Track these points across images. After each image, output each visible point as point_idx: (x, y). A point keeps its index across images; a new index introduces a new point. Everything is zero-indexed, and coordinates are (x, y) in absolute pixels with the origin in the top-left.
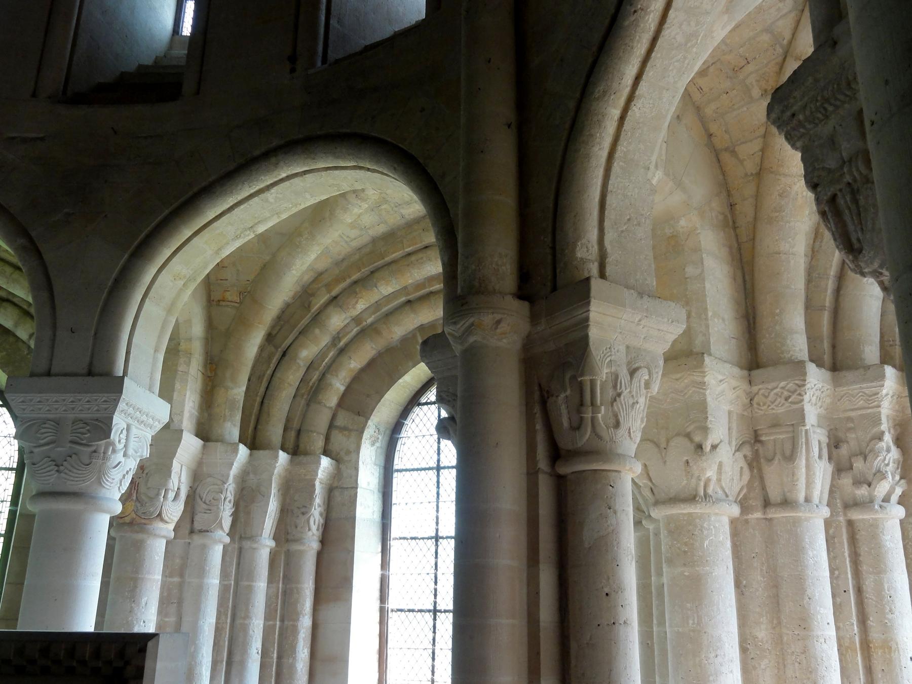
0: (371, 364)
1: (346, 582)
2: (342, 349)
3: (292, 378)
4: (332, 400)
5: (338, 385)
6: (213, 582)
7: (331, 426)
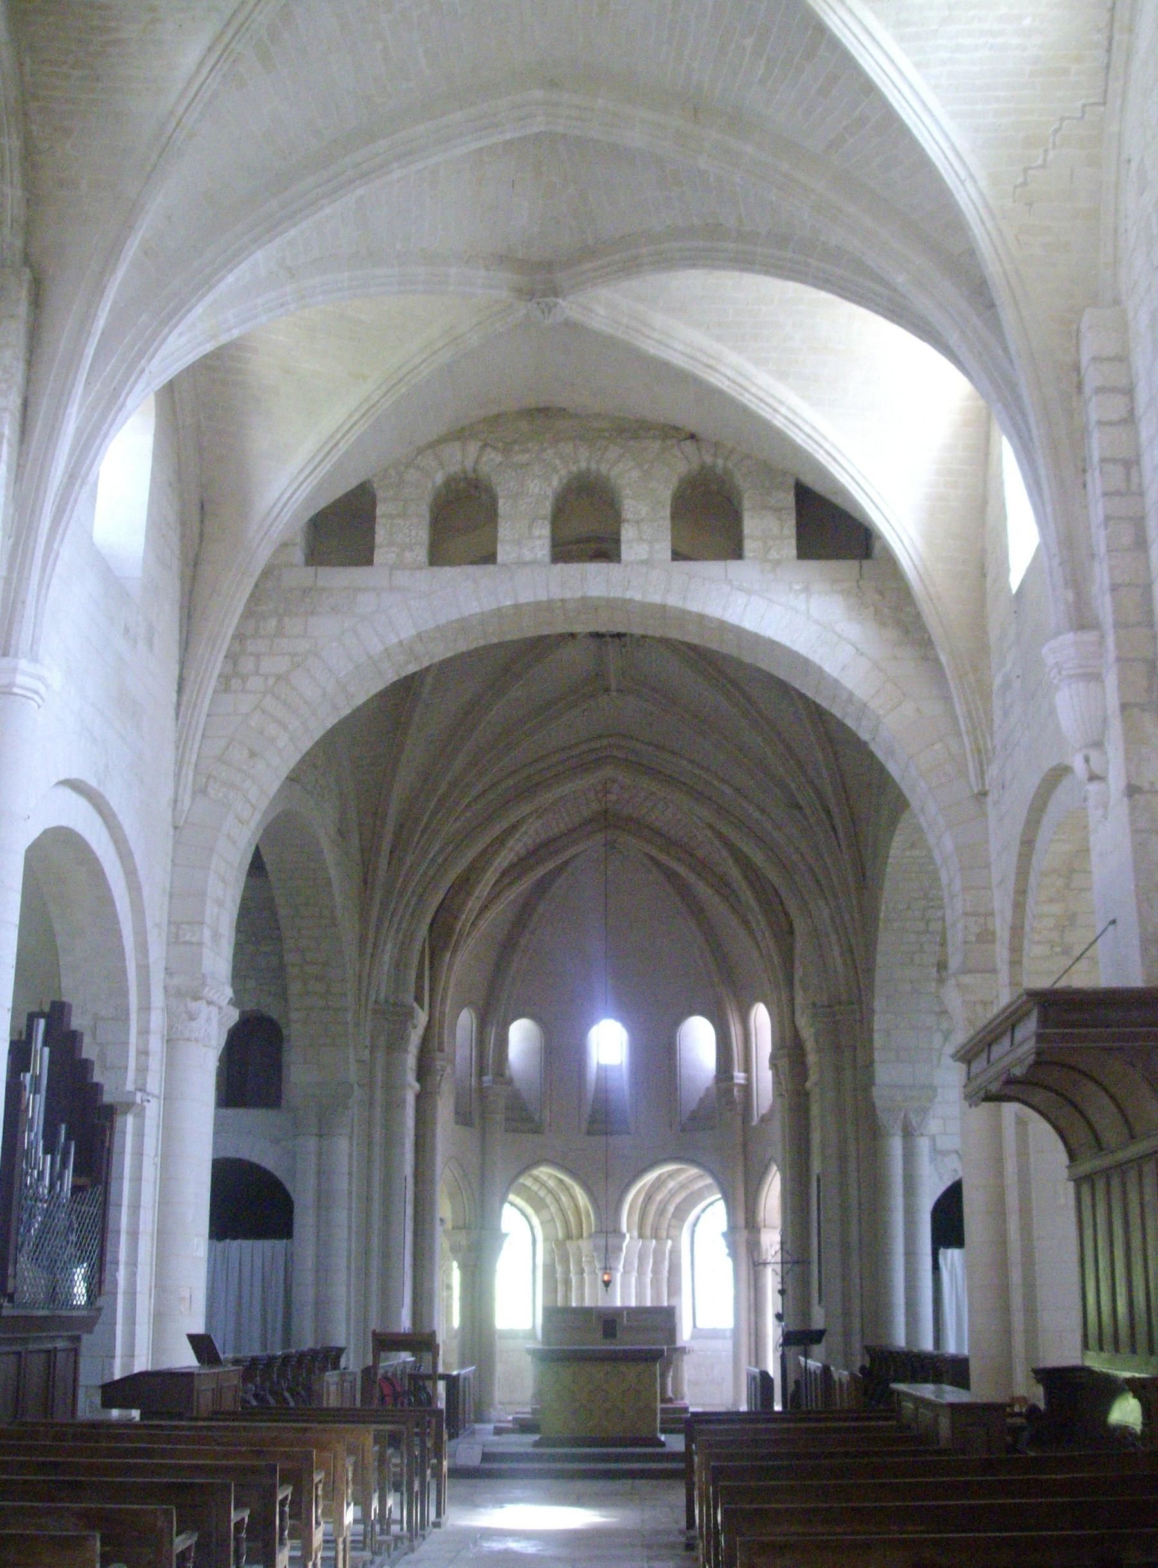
0: (684, 1200)
1: (680, 1289)
2: (673, 1194)
3: (653, 1209)
4: (669, 1215)
5: (671, 1208)
6: (633, 1291)
7: (669, 1226)
